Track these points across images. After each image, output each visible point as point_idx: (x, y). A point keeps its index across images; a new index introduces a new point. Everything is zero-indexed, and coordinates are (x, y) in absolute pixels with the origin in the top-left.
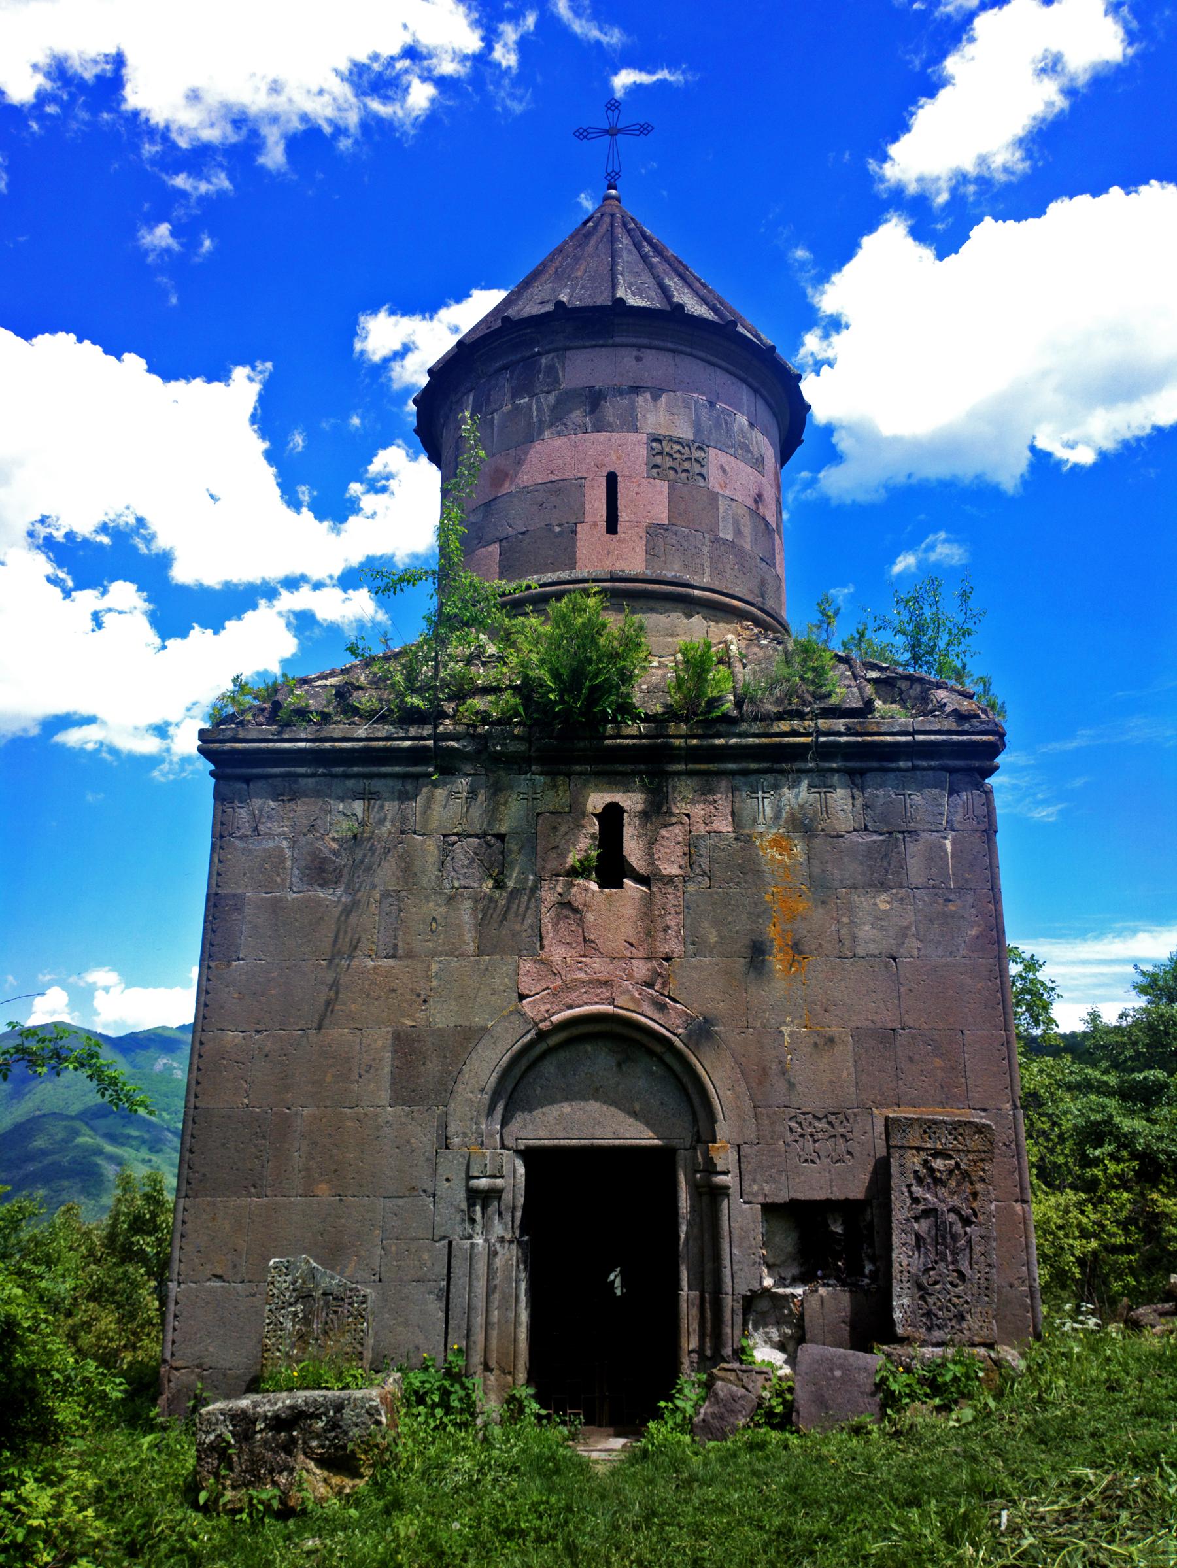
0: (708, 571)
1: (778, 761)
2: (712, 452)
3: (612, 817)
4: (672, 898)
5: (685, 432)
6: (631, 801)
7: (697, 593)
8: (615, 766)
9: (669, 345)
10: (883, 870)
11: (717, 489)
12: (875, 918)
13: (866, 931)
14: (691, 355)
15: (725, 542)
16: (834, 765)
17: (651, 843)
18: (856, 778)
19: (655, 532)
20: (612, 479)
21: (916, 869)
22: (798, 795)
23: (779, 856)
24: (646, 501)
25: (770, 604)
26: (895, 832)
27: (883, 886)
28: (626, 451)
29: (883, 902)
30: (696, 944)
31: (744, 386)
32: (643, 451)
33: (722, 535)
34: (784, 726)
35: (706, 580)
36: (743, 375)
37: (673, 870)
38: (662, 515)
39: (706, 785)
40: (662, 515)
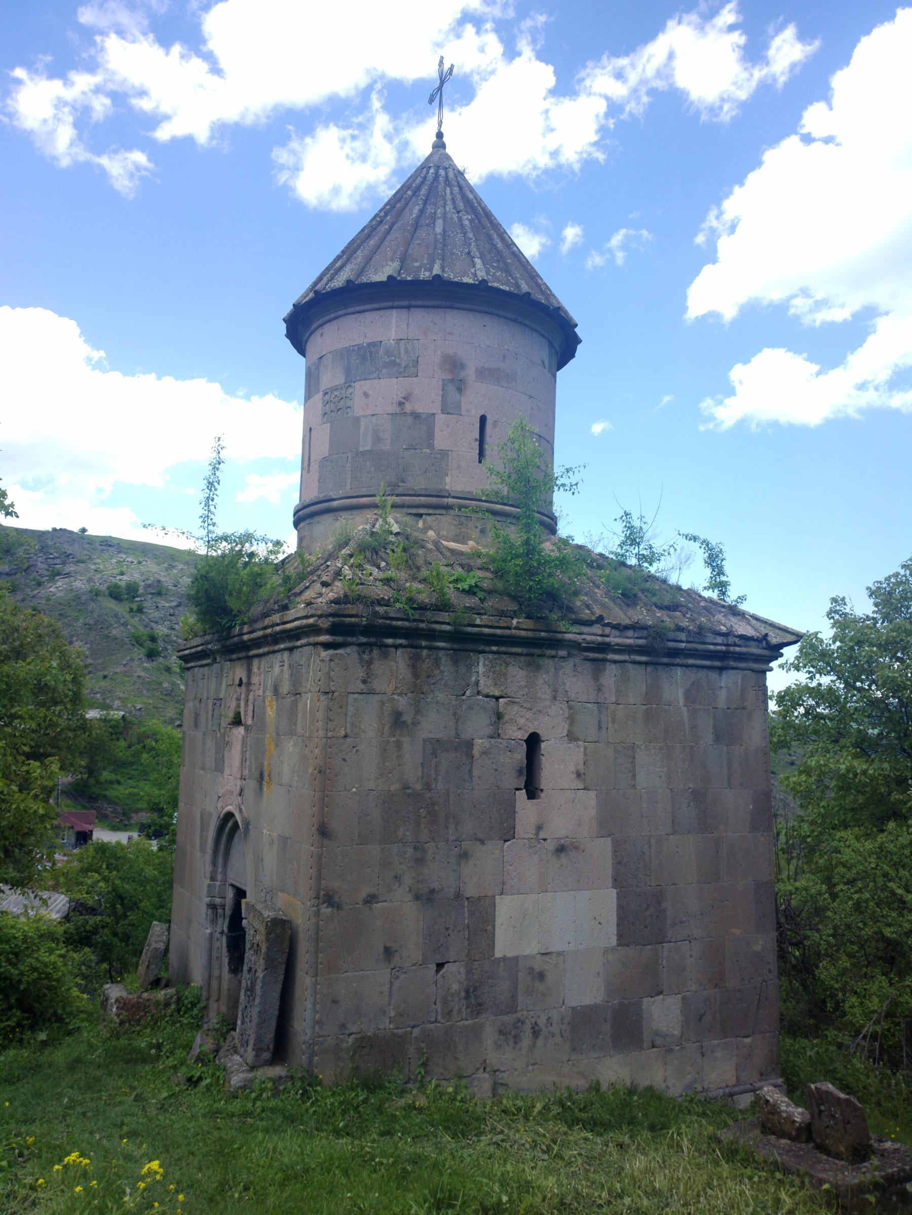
0: (349, 481)
2: (357, 385)
7: (335, 504)
9: (333, 315)
11: (361, 413)
14: (346, 314)
15: (363, 453)
16: (282, 646)
25: (417, 482)
31: (394, 311)
32: (320, 405)
33: (361, 449)
34: (267, 622)
35: (348, 490)
36: (390, 304)
37: (249, 722)
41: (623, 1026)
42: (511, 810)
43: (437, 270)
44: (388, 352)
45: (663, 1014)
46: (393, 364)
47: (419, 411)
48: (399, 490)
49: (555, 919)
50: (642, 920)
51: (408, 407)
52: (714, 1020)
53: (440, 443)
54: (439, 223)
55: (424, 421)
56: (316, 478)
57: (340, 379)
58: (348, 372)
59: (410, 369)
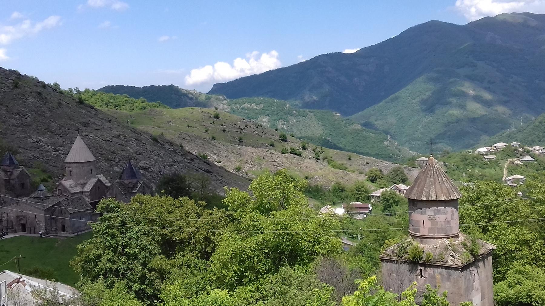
1: (437, 267)
3: (421, 270)
5: (433, 214)
6: (422, 268)
8: (421, 265)
10: (448, 279)
12: (448, 284)
18: (446, 269)
19: (429, 229)
21: (452, 280)
22: (440, 270)
23: (438, 277)
26: (449, 275)
27: (448, 281)
28: (424, 217)
29: (448, 283)
38: (430, 226)
40: (430, 226)
42: (473, 285)
50: (483, 298)
53: (451, 225)
55: (449, 222)
57: (433, 214)
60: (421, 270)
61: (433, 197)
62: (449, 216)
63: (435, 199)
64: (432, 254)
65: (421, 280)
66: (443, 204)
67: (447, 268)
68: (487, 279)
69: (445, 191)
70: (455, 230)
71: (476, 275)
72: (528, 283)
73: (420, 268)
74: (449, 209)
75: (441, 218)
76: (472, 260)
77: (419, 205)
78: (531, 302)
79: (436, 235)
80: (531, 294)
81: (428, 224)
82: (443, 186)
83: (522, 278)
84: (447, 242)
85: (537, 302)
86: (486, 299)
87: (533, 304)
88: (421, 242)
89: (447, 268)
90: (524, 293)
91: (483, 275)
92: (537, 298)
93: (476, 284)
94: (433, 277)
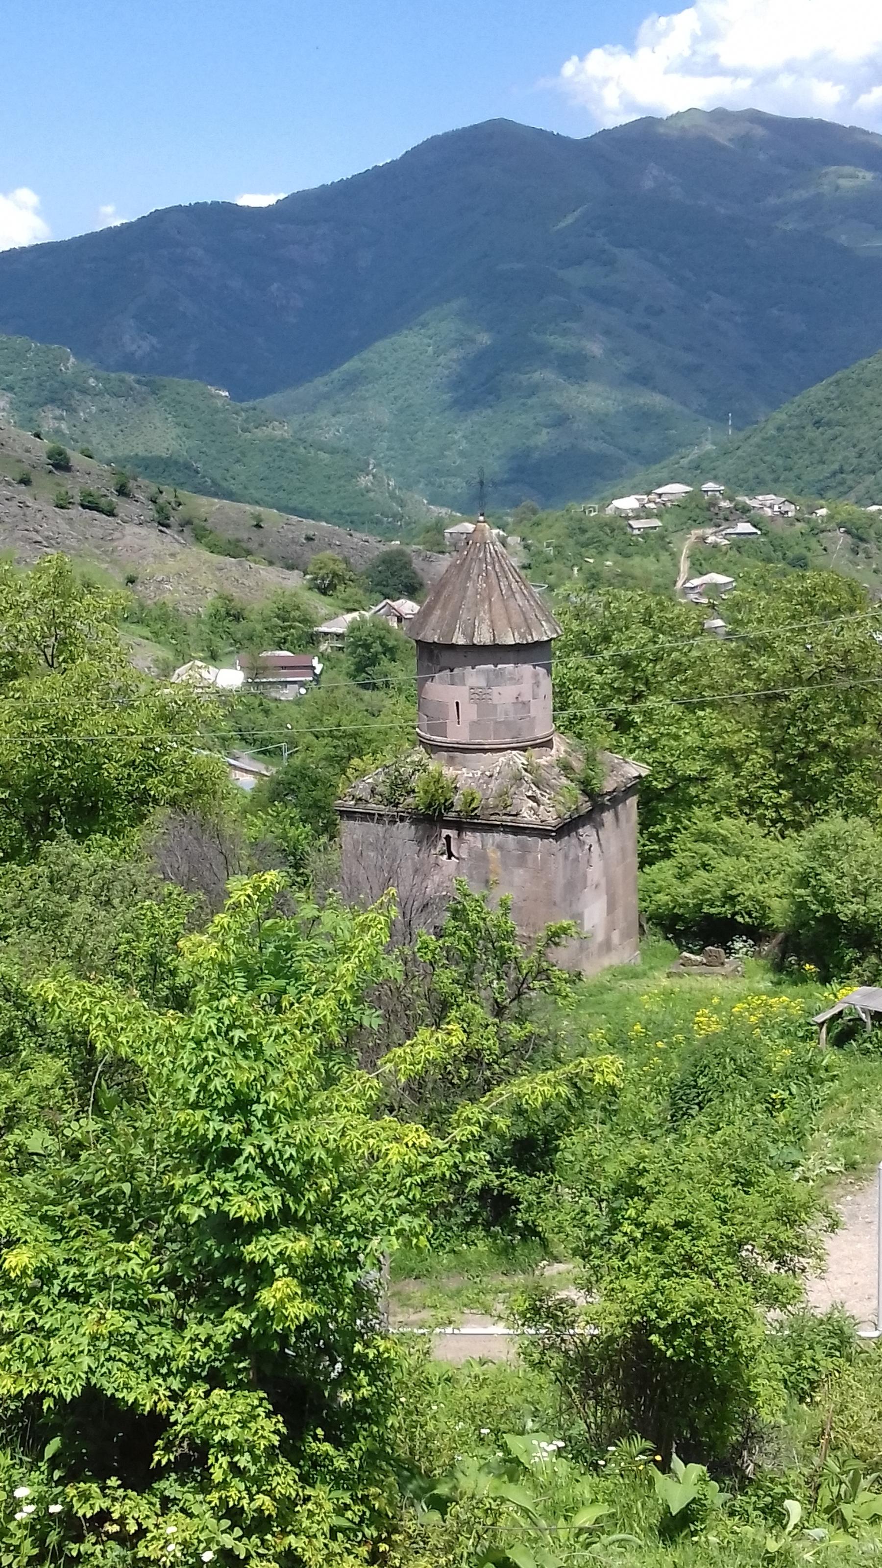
1: (491, 828)
3: (448, 838)
4: (464, 864)
6: (452, 833)
10: (521, 861)
12: (520, 875)
13: (516, 879)
17: (459, 847)
18: (515, 834)
19: (473, 724)
20: (457, 703)
21: (530, 864)
22: (498, 837)
23: (494, 855)
24: (470, 712)
26: (525, 850)
28: (460, 693)
29: (521, 871)
30: (471, 877)
34: (493, 818)
38: (475, 718)
39: (474, 830)
40: (475, 718)
41: (607, 946)
42: (585, 876)
43: (536, 639)
44: (510, 673)
45: (616, 937)
46: (511, 679)
47: (525, 699)
48: (520, 739)
49: (594, 913)
51: (520, 699)
52: (625, 936)
53: (532, 714)
54: (517, 595)
56: (467, 730)
57: (483, 684)
58: (488, 681)
59: (519, 681)
60: (448, 838)
61: (483, 637)
62: (526, 689)
63: (488, 642)
64: (478, 795)
65: (448, 865)
66: (511, 655)
67: (517, 830)
68: (624, 858)
69: (517, 619)
70: (543, 728)
71: (595, 848)
72: (727, 865)
73: (445, 832)
74: (527, 669)
75: (504, 695)
76: (586, 807)
77: (446, 658)
78: (735, 914)
79: (490, 741)
80: (733, 892)
81: (470, 712)
82: (512, 603)
83: (712, 852)
84: (519, 759)
85: (749, 914)
86: (620, 912)
87: (739, 919)
88: (451, 762)
89: (517, 830)
90: (717, 892)
91: (613, 848)
92: (749, 904)
93: (595, 873)
94: (481, 858)
